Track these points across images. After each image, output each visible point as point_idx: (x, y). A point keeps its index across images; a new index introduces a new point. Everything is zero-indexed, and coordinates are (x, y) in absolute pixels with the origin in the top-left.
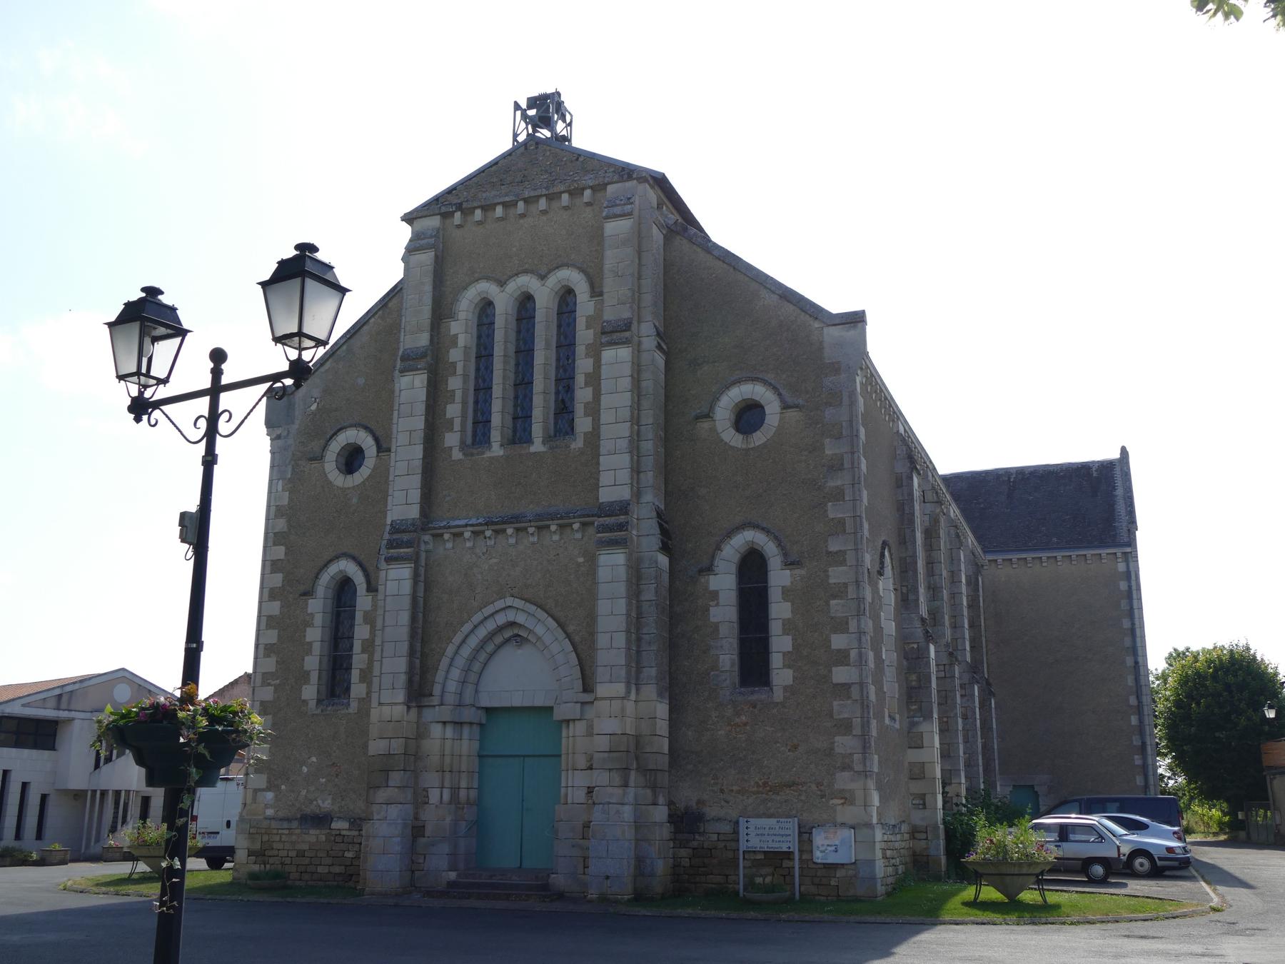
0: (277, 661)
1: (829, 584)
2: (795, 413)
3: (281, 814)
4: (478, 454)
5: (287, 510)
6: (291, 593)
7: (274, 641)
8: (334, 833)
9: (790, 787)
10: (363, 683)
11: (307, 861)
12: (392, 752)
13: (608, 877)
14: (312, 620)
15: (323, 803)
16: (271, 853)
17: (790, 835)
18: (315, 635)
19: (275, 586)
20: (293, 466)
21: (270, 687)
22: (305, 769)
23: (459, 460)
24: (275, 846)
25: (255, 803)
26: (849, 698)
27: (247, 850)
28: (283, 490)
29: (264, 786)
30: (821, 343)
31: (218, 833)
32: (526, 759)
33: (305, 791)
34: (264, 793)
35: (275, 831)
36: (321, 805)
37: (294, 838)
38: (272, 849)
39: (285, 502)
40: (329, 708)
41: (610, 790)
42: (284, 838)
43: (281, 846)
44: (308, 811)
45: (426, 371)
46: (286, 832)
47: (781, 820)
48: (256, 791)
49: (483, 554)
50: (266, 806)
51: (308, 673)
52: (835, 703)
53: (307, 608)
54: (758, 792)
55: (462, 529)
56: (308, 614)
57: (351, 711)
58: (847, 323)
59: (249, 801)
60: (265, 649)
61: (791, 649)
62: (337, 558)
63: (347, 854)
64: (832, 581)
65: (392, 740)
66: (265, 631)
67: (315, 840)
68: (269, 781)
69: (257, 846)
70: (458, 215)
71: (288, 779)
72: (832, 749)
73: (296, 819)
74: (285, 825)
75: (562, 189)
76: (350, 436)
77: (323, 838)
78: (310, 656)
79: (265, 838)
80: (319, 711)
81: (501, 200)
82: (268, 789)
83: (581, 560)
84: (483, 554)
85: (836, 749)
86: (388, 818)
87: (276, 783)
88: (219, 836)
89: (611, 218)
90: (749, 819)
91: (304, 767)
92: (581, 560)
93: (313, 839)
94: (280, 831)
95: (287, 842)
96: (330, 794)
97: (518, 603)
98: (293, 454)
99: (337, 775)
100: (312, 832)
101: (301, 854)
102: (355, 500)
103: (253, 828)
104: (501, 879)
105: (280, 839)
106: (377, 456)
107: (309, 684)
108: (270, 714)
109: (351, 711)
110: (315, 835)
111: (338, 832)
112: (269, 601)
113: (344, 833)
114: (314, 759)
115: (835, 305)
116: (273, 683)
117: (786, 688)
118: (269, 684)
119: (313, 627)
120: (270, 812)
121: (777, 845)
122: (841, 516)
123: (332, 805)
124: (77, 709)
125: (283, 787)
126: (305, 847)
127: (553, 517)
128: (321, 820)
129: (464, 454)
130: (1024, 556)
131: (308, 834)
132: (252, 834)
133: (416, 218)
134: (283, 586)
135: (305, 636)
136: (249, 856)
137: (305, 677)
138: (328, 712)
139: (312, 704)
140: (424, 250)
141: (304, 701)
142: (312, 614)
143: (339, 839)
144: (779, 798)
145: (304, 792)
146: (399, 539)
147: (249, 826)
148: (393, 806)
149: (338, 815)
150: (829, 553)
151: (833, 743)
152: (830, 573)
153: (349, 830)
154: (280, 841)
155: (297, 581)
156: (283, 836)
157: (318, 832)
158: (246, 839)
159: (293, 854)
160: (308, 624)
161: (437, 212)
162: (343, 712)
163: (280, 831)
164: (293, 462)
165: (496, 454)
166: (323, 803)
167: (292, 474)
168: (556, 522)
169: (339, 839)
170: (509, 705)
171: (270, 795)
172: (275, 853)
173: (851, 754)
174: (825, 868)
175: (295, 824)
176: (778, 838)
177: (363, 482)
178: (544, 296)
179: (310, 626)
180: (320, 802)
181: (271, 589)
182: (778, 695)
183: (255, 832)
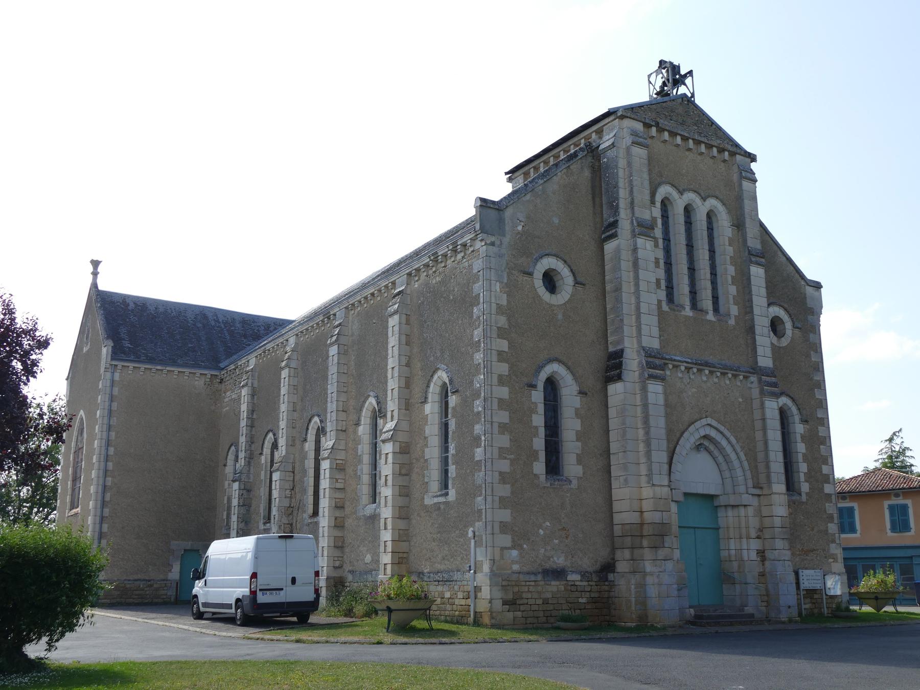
0: (510, 439)
1: (819, 436)
2: (797, 332)
3: (525, 569)
4: (677, 311)
5: (506, 310)
6: (518, 383)
7: (506, 420)
8: (570, 583)
9: (812, 551)
10: (580, 465)
11: (551, 607)
12: (664, 522)
13: (789, 607)
14: (536, 408)
15: (558, 559)
16: (521, 602)
17: (819, 580)
18: (539, 420)
19: (503, 374)
20: (508, 273)
21: (506, 461)
22: (541, 532)
23: (710, 320)
24: (524, 595)
25: (503, 559)
26: (831, 502)
27: (501, 600)
28: (501, 292)
29: (509, 544)
30: (805, 294)
31: (282, 589)
32: (696, 529)
33: (544, 550)
34: (510, 551)
35: (523, 583)
36: (557, 561)
37: (539, 588)
38: (522, 598)
39: (504, 302)
40: (556, 483)
41: (784, 551)
42: (531, 589)
43: (529, 596)
44: (547, 566)
45: (653, 240)
46: (533, 583)
47: (816, 571)
48: (502, 549)
49: (688, 383)
50: (513, 562)
51: (537, 452)
52: (827, 504)
53: (531, 397)
54: (800, 555)
55: (680, 363)
56: (533, 403)
57: (572, 486)
58: (816, 287)
59: (497, 558)
60: (499, 427)
61: (807, 472)
62: (550, 361)
63: (581, 600)
64: (820, 435)
65: (664, 513)
66: (498, 411)
67: (556, 590)
68: (513, 541)
69: (510, 596)
70: (654, 129)
71: (529, 540)
72: (827, 531)
73: (539, 573)
74: (533, 578)
75: (716, 144)
76: (548, 263)
77: (562, 588)
78: (537, 439)
79: (516, 589)
80: (548, 485)
81: (682, 133)
82: (513, 547)
83: (740, 400)
84: (688, 383)
85: (829, 530)
86: (666, 571)
87: (519, 542)
88: (282, 593)
89: (746, 179)
90: (803, 570)
91: (541, 531)
92: (740, 400)
93: (555, 589)
94: (528, 583)
95: (534, 592)
96: (563, 553)
97: (714, 423)
98: (507, 264)
99: (567, 537)
100: (553, 583)
101: (546, 602)
102: (560, 317)
103: (504, 581)
104: (721, 612)
105: (528, 590)
106: (574, 286)
107: (538, 461)
108: (509, 484)
109: (572, 486)
110: (555, 586)
111: (573, 583)
112: (499, 385)
113: (577, 583)
114: (548, 524)
115: (810, 275)
116: (508, 457)
117: (807, 494)
118: (506, 458)
119: (537, 414)
120: (516, 567)
121: (814, 585)
122: (820, 398)
123: (565, 561)
124: (226, 455)
125: (525, 546)
126: (549, 595)
127: (707, 364)
128: (558, 574)
129: (669, 308)
130: (193, 371)
131: (550, 585)
132: (505, 586)
133: (627, 117)
134: (510, 374)
135: (531, 421)
136: (503, 605)
137: (534, 455)
138: (555, 486)
139: (543, 478)
140: (642, 146)
141: (535, 475)
142: (535, 403)
143: (573, 589)
144: (808, 558)
145: (542, 551)
146: (652, 362)
147: (501, 579)
148: (669, 561)
149: (570, 569)
150: (818, 418)
151: (827, 527)
152: (819, 430)
153: (581, 581)
154: (529, 591)
155: (521, 373)
156: (531, 587)
157: (558, 583)
158: (499, 590)
159: (540, 602)
160: (533, 411)
161: (643, 120)
162: (566, 487)
163: (528, 583)
164: (507, 270)
165: (687, 314)
166: (558, 559)
167: (507, 280)
168: (732, 372)
169: (573, 589)
170: (696, 492)
171: (515, 553)
172: (526, 601)
173: (835, 534)
174: (831, 598)
175: (539, 577)
176: (815, 581)
177: (564, 303)
178: (701, 209)
179: (534, 413)
180: (555, 559)
181: (499, 375)
182: (804, 498)
183: (507, 584)
